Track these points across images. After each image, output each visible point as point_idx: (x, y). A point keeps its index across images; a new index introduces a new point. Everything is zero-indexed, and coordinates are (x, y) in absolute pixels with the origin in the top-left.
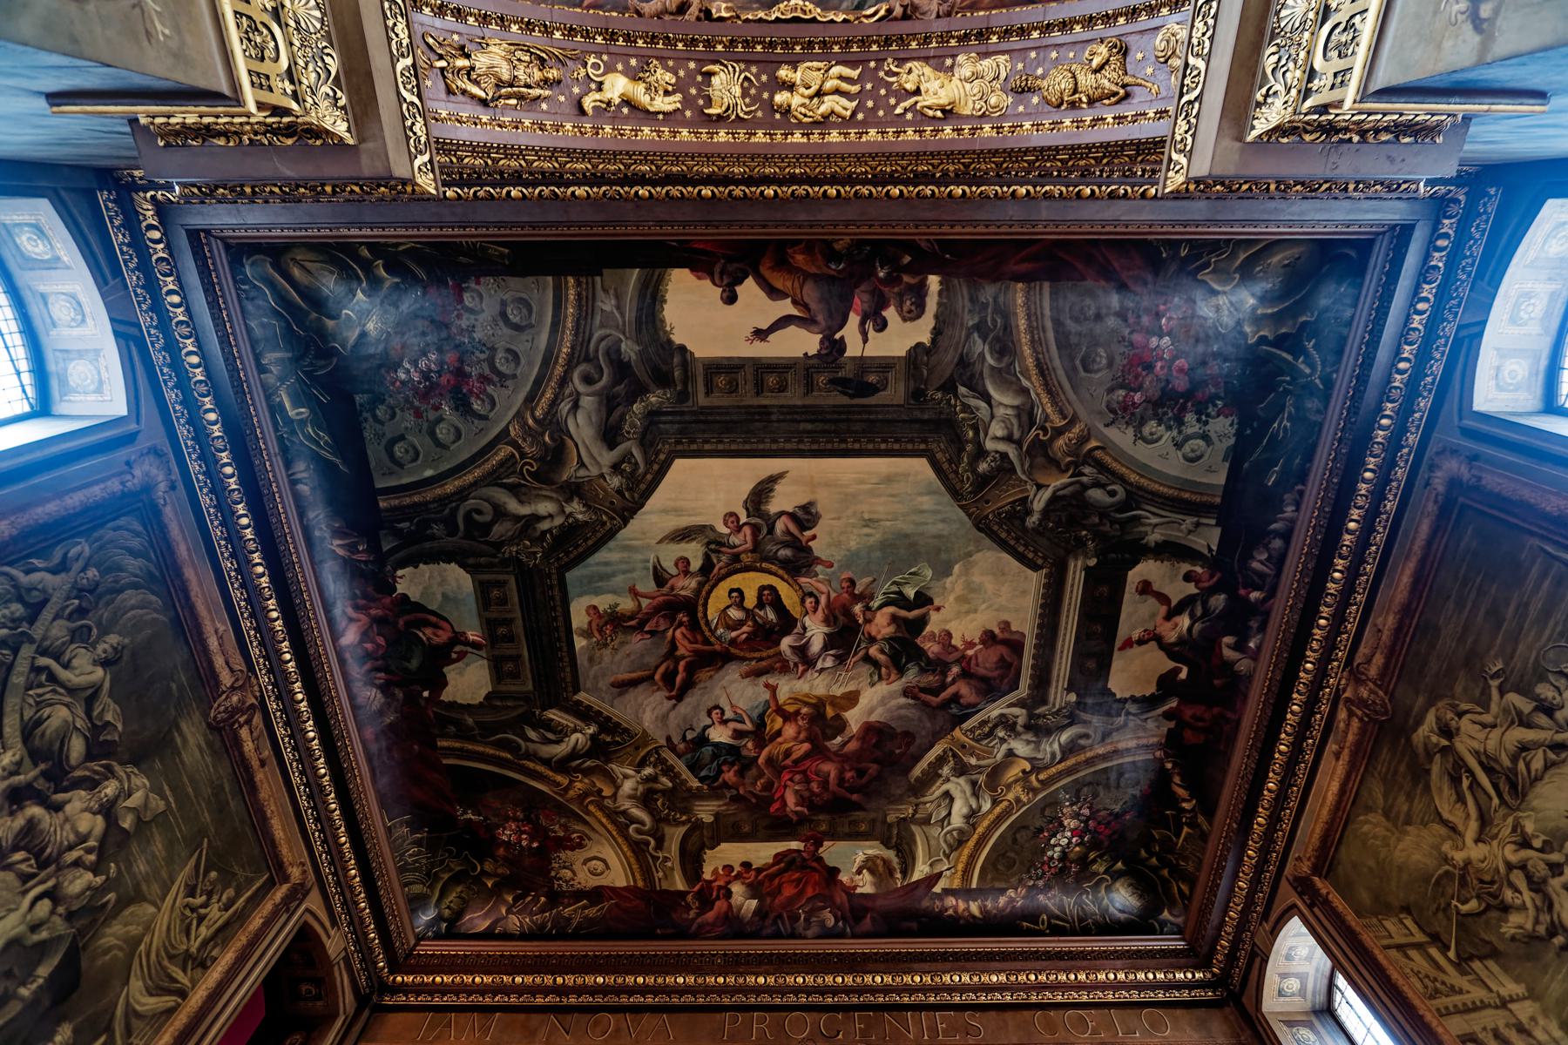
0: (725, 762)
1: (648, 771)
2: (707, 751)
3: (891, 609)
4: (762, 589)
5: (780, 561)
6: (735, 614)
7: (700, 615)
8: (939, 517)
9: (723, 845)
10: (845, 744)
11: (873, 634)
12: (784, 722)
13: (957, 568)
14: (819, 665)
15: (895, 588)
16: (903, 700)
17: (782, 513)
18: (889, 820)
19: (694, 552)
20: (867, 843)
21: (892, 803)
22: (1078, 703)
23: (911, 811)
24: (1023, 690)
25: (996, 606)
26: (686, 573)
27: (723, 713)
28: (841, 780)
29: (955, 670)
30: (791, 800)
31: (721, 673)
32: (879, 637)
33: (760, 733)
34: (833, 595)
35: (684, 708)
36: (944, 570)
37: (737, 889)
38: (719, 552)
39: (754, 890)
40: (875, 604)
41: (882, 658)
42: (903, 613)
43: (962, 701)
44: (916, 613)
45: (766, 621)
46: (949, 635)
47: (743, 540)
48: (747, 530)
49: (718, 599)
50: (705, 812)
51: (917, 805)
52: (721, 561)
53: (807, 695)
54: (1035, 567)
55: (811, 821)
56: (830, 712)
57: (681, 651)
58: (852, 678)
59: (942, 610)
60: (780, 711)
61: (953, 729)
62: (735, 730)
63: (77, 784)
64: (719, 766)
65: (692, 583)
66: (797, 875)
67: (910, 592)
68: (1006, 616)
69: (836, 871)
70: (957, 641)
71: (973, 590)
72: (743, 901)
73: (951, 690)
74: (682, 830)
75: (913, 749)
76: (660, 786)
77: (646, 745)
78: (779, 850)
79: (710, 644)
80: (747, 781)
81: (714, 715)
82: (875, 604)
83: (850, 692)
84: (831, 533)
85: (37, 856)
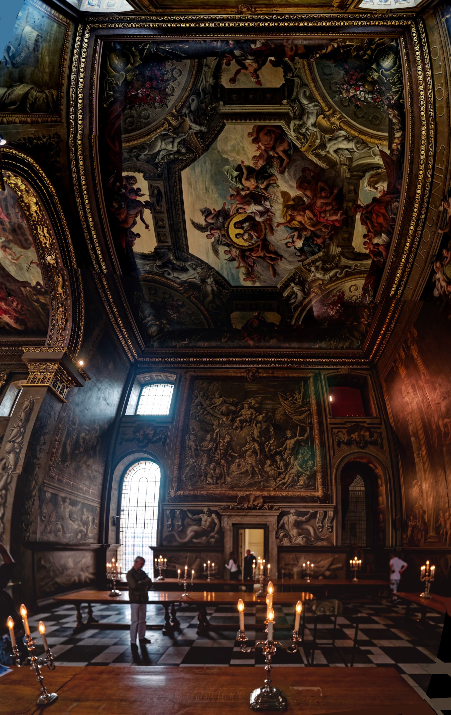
0: (312, 242)
1: (313, 269)
2: (306, 248)
3: (243, 181)
4: (235, 227)
5: (224, 221)
6: (246, 237)
7: (247, 248)
8: (203, 165)
9: (353, 244)
10: (307, 196)
11: (254, 187)
12: (295, 220)
13: (225, 156)
14: (269, 207)
15: (234, 180)
16: (286, 174)
17: (205, 220)
18: (349, 176)
19: (222, 249)
20: (361, 185)
21: (339, 176)
22: (289, 98)
23: (344, 167)
24: (282, 123)
25: (241, 139)
26: (230, 251)
27: (289, 242)
28: (325, 198)
29: (271, 153)
30: (334, 218)
31: (271, 242)
32: (256, 184)
33: (300, 229)
34: (237, 202)
35: (286, 255)
36: (226, 161)
37: (376, 241)
38: (221, 242)
39: (378, 234)
40: (241, 186)
41: (265, 183)
42: (245, 176)
43: (287, 149)
44: (245, 171)
45: (248, 227)
46: (254, 157)
47: (217, 234)
48: (212, 232)
49: (240, 242)
50: (335, 250)
51: (341, 164)
52: (225, 240)
53: (283, 212)
54: (224, 125)
55: (346, 209)
56: (291, 203)
57: (262, 254)
58: (275, 195)
59: (243, 160)
60: (290, 222)
61: (301, 151)
62: (298, 238)
63: (240, 411)
64: (314, 244)
65: (234, 250)
66: (374, 216)
67: (236, 173)
68: (246, 135)
69: (375, 199)
70: (258, 154)
71: (234, 149)
72: (383, 239)
73: (281, 154)
74: (343, 259)
75: (311, 168)
76: (321, 266)
77: (301, 268)
78: (360, 222)
79: (259, 245)
80: (322, 234)
81: (290, 245)
82: (241, 186)
83: (282, 195)
84: (212, 204)
85: (247, 421)
